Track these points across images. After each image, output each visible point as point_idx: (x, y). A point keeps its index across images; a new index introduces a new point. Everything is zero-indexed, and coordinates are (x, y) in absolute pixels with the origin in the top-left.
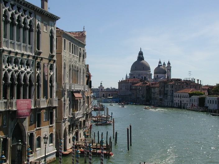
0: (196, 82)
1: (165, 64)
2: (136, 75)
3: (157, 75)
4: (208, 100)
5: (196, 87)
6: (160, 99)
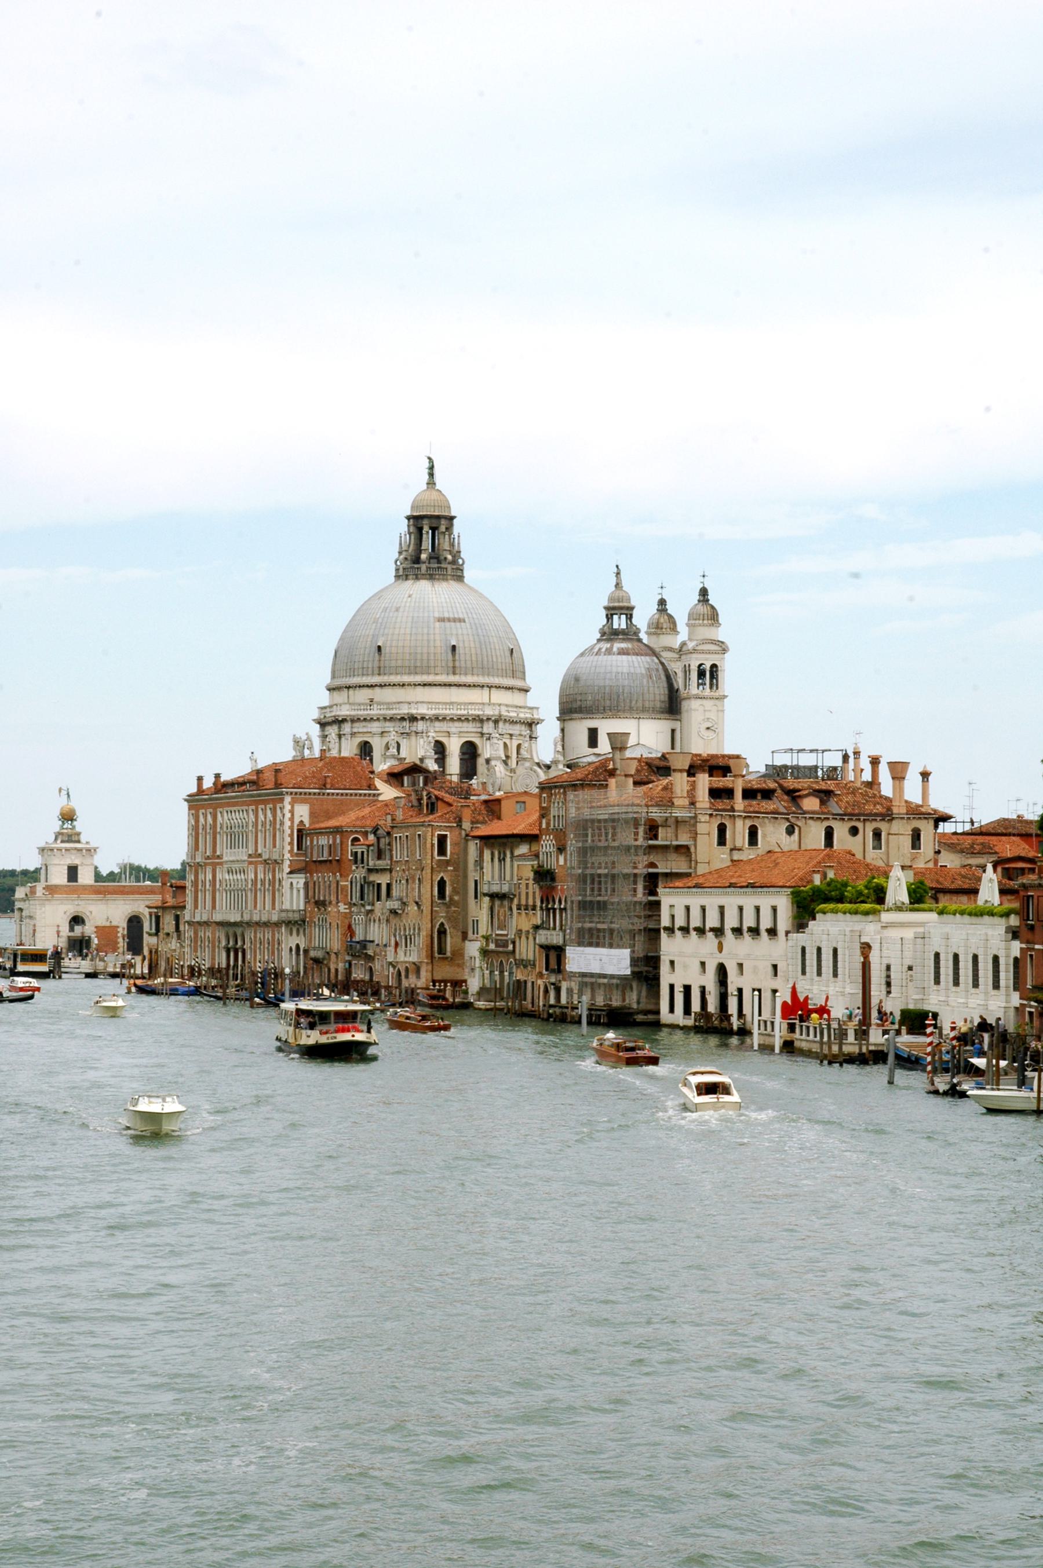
0: (887, 787)
1: (670, 617)
2: (375, 727)
3: (592, 724)
4: (937, 956)
5: (877, 835)
6: (547, 948)
